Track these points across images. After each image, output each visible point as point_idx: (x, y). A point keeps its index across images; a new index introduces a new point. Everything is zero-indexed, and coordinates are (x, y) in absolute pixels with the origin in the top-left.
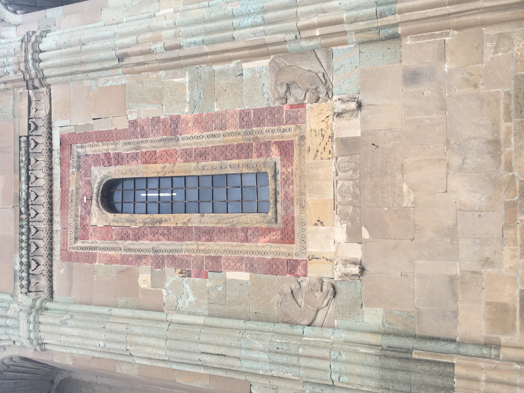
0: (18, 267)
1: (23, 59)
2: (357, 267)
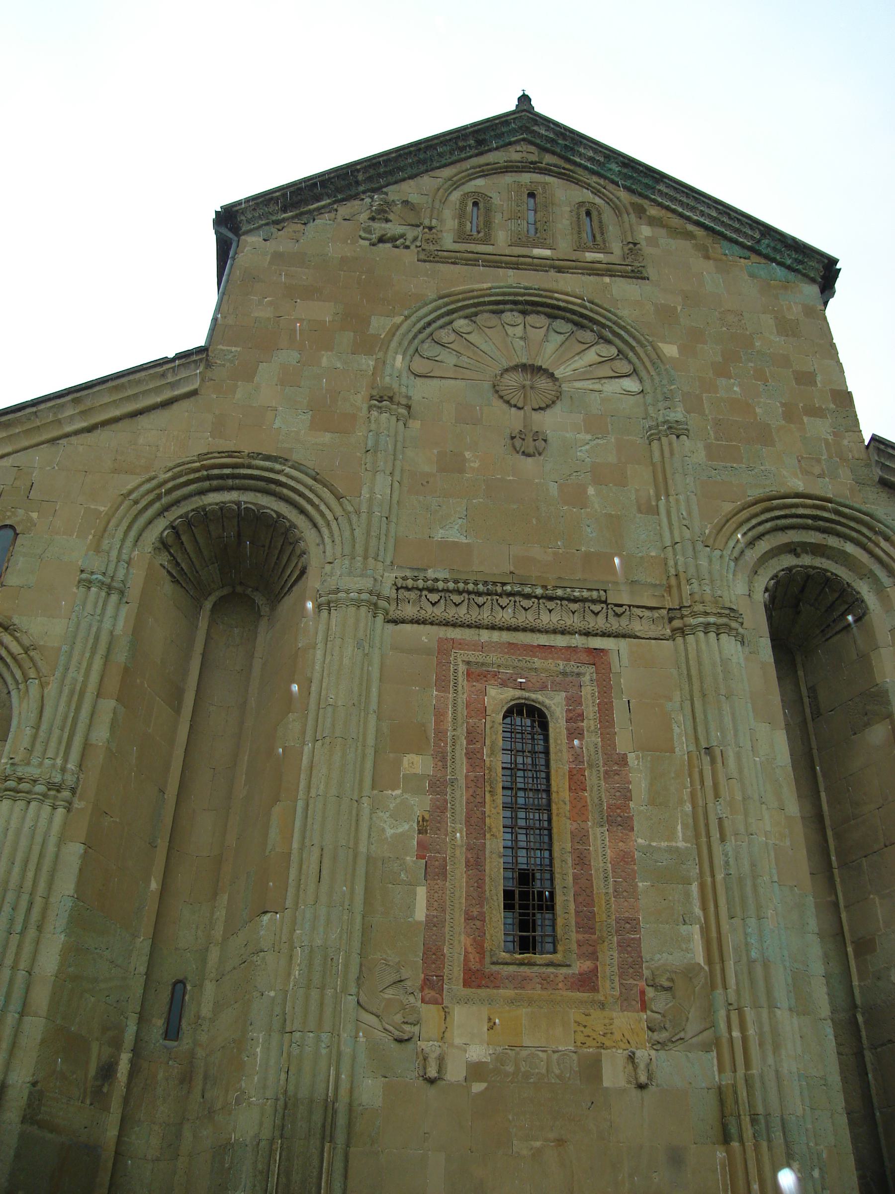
0: (430, 574)
1: (709, 610)
2: (436, 1075)
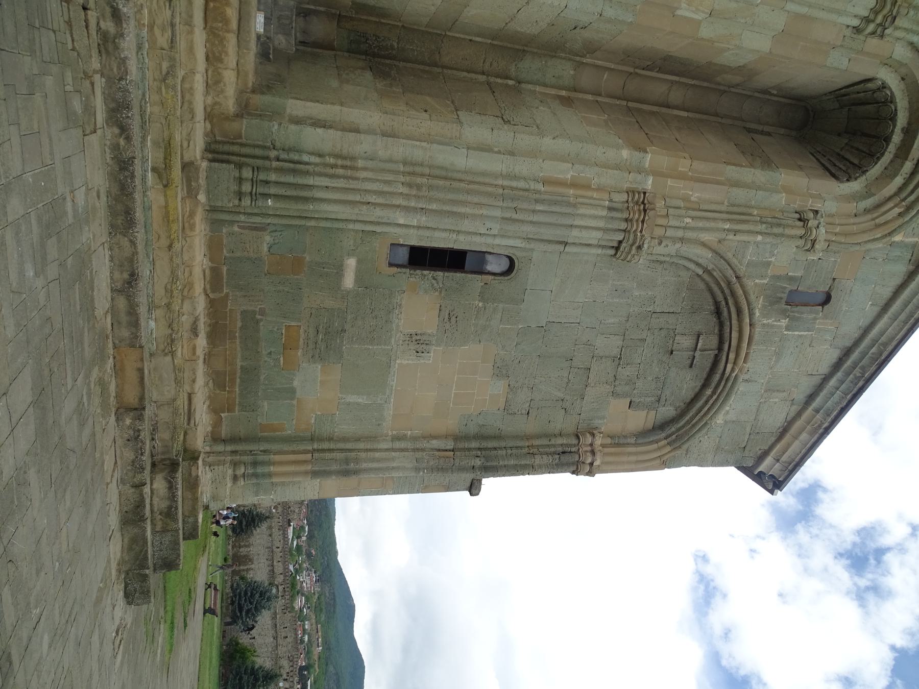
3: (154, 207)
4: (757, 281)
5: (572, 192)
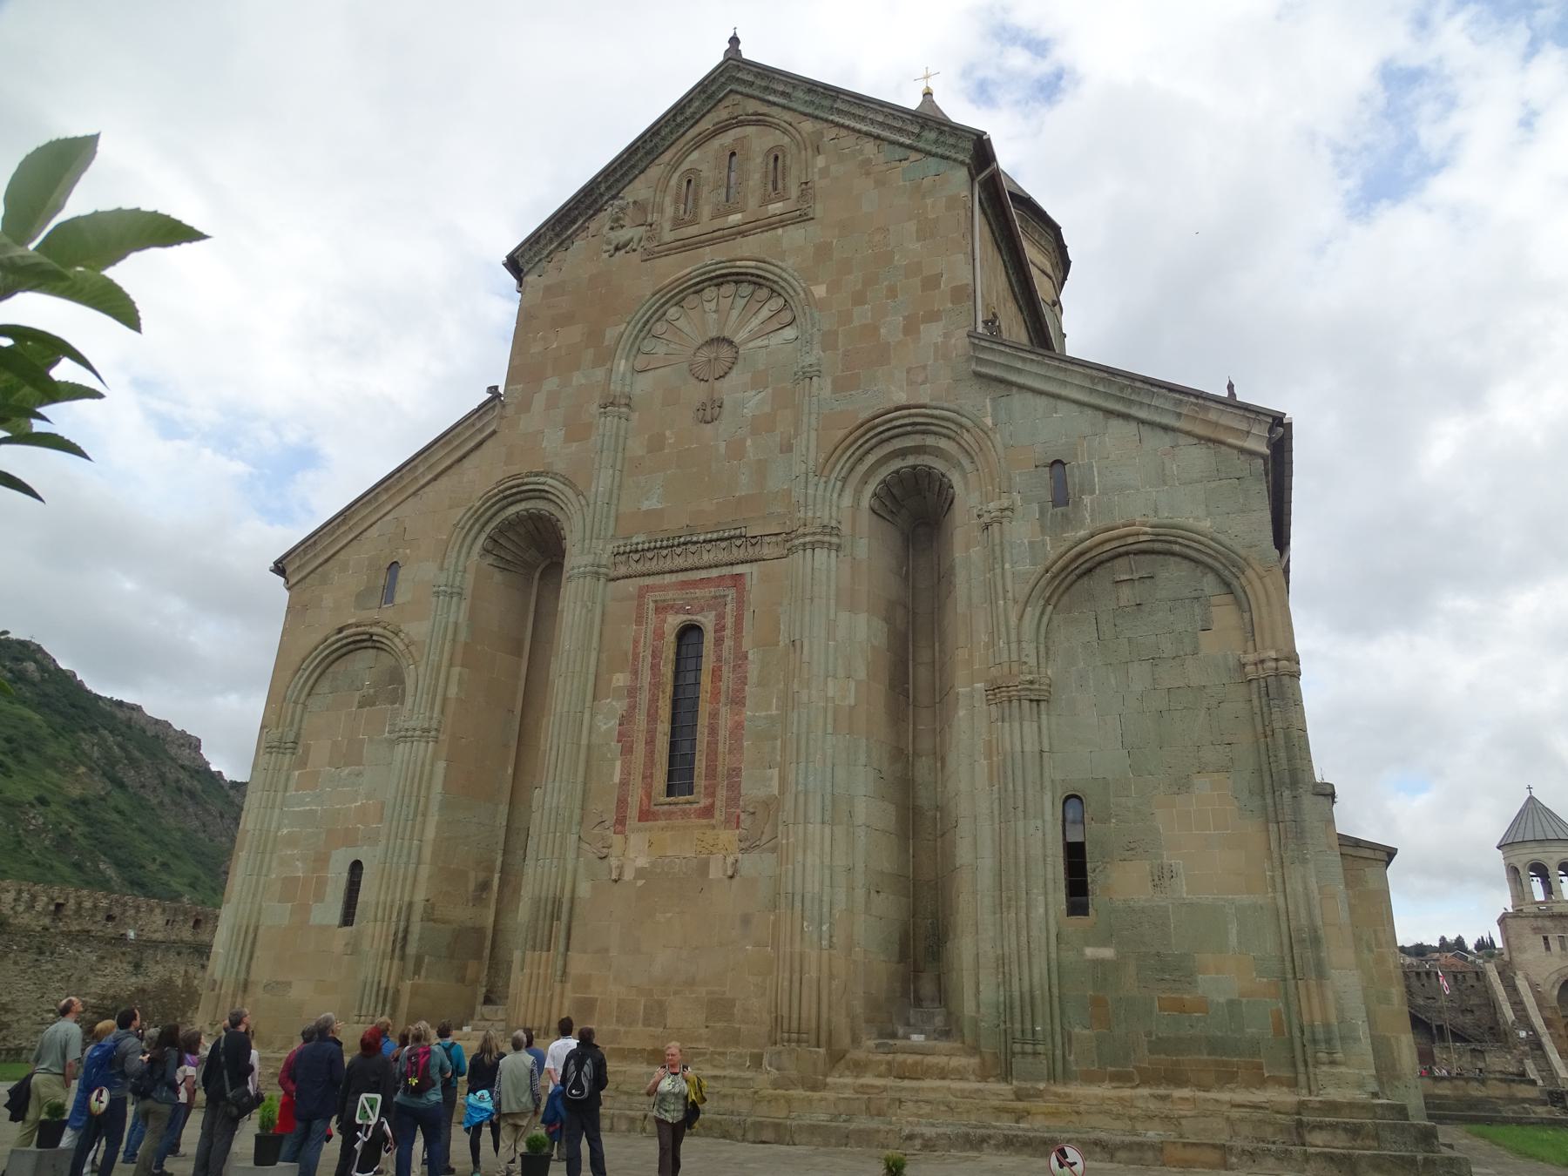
0: (635, 540)
3: (1047, 1123)
4: (1049, 548)
5: (995, 759)
